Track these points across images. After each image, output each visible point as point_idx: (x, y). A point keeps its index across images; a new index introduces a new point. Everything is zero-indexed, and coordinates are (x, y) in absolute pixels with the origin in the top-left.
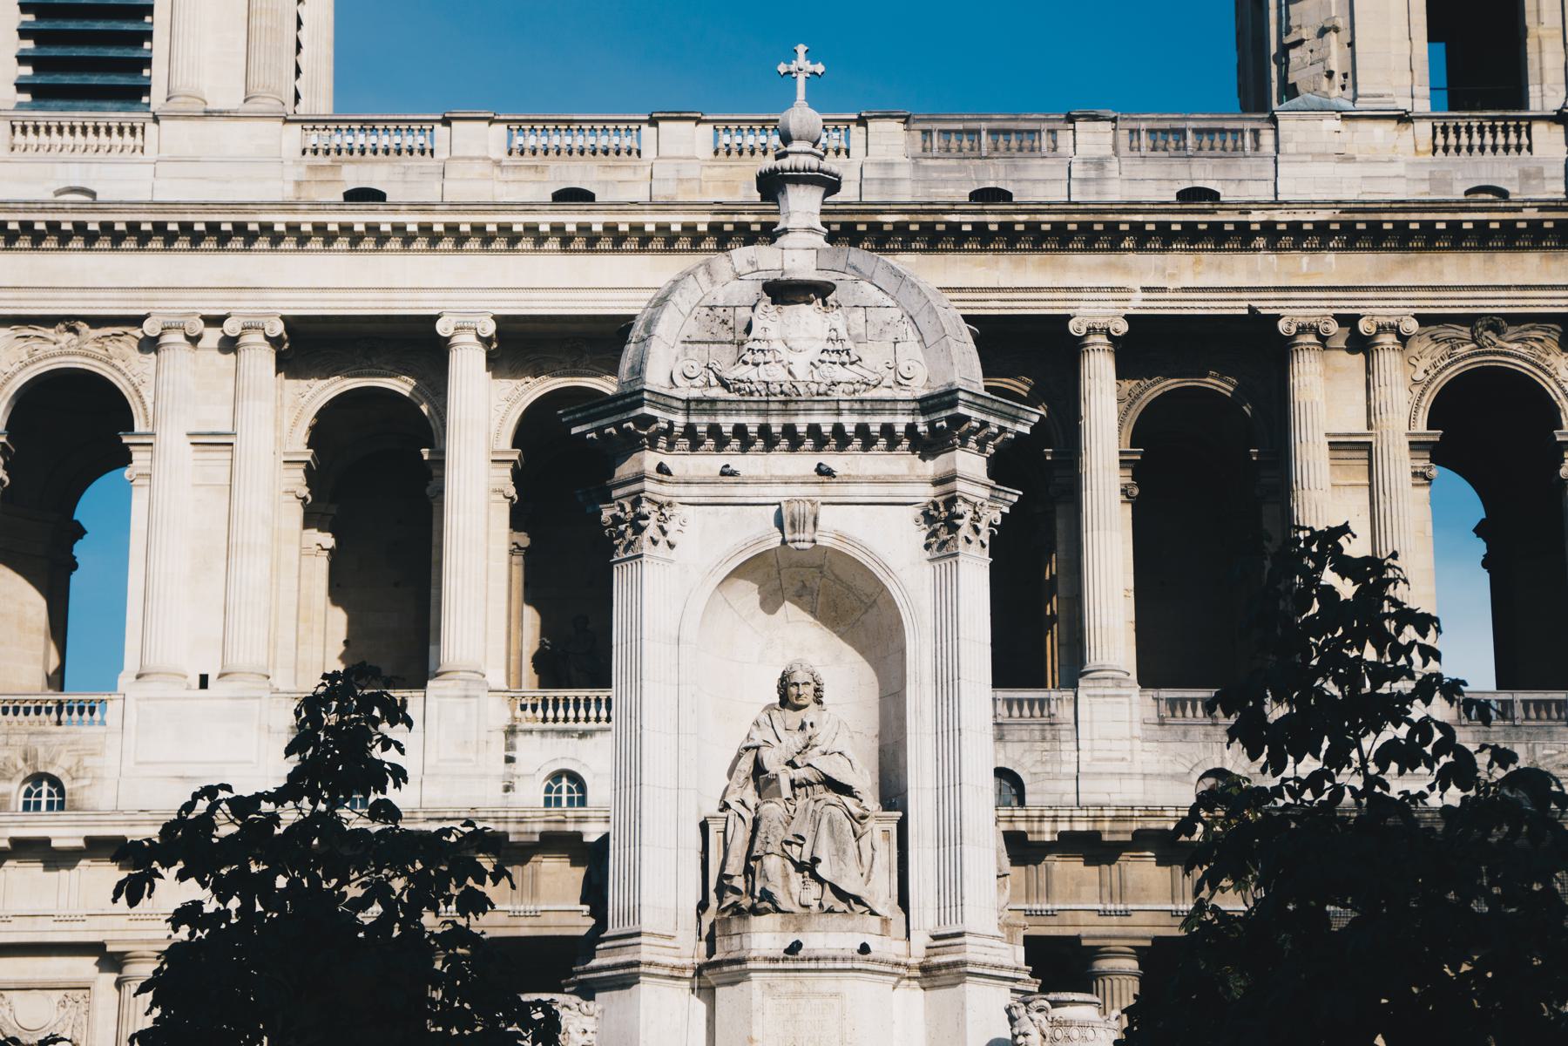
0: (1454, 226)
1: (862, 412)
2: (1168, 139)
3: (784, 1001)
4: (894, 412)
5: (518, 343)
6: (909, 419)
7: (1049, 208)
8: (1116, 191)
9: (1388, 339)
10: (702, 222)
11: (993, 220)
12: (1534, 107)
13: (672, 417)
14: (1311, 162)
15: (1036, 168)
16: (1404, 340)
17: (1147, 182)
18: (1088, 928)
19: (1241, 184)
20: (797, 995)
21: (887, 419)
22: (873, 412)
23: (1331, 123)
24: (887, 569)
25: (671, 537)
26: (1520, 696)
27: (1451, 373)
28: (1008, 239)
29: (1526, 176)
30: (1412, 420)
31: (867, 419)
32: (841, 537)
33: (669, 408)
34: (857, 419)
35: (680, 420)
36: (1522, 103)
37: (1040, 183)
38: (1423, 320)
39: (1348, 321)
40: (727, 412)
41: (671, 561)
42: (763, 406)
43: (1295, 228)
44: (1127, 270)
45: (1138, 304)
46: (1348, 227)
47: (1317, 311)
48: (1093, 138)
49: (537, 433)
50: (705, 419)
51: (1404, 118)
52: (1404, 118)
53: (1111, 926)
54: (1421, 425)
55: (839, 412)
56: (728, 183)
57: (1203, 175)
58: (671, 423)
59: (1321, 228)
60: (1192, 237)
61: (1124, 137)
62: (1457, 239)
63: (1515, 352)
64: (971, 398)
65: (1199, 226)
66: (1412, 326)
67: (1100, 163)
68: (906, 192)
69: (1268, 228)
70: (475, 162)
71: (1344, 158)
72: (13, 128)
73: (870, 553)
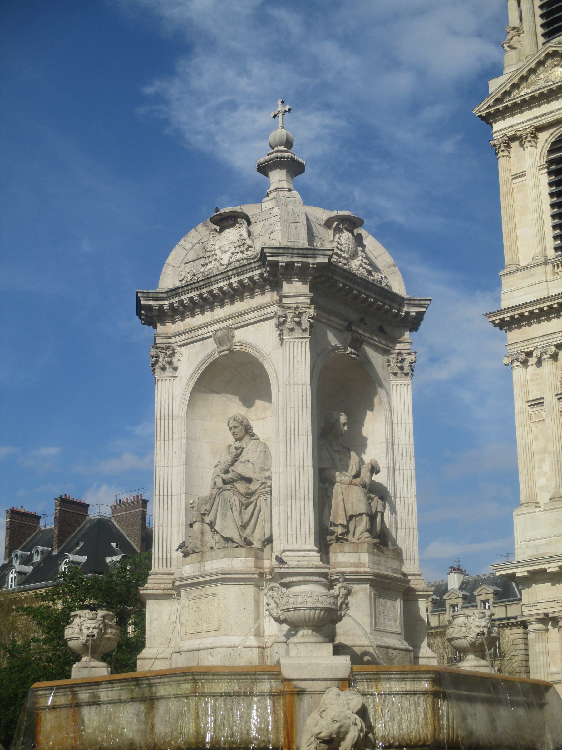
1: (238, 274)
3: (194, 601)
4: (252, 270)
6: (259, 272)
13: (161, 303)
20: (198, 597)
21: (250, 275)
22: (243, 273)
24: (262, 355)
25: (175, 364)
31: (242, 277)
32: (243, 344)
33: (158, 299)
34: (237, 279)
35: (166, 303)
40: (184, 293)
41: (176, 377)
42: (197, 285)
50: (177, 299)
55: (229, 278)
58: (161, 307)
64: (274, 251)
72: (554, 266)
73: (255, 349)
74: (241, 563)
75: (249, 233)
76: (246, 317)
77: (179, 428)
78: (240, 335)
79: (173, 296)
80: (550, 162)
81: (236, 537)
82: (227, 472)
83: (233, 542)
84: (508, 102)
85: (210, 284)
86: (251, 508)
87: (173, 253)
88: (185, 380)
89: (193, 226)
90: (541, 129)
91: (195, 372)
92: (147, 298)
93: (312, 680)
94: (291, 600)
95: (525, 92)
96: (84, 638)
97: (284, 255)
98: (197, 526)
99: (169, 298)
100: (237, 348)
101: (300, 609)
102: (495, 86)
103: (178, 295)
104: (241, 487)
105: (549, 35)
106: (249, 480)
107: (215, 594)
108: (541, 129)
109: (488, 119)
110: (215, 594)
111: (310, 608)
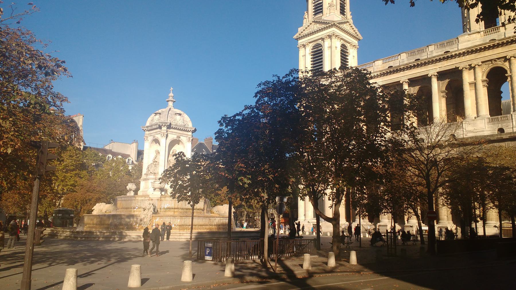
0: (485, 47)
2: (442, 45)
7: (426, 59)
8: (435, 54)
9: (477, 66)
15: (424, 54)
19: (453, 49)
27: (489, 69)
29: (499, 36)
30: (482, 77)
37: (424, 57)
38: (482, 62)
39: (470, 65)
44: (437, 65)
45: (439, 70)
47: (466, 65)
48: (431, 48)
51: (479, 32)
52: (479, 32)
56: (383, 67)
57: (448, 49)
60: (448, 58)
61: (436, 47)
62: (489, 48)
63: (500, 64)
66: (481, 63)
67: (432, 51)
68: (406, 62)
71: (469, 41)
80: (312, 52)
84: (302, 35)
90: (310, 43)
95: (306, 32)
102: (300, 29)
105: (315, 15)
108: (310, 43)
109: (297, 39)
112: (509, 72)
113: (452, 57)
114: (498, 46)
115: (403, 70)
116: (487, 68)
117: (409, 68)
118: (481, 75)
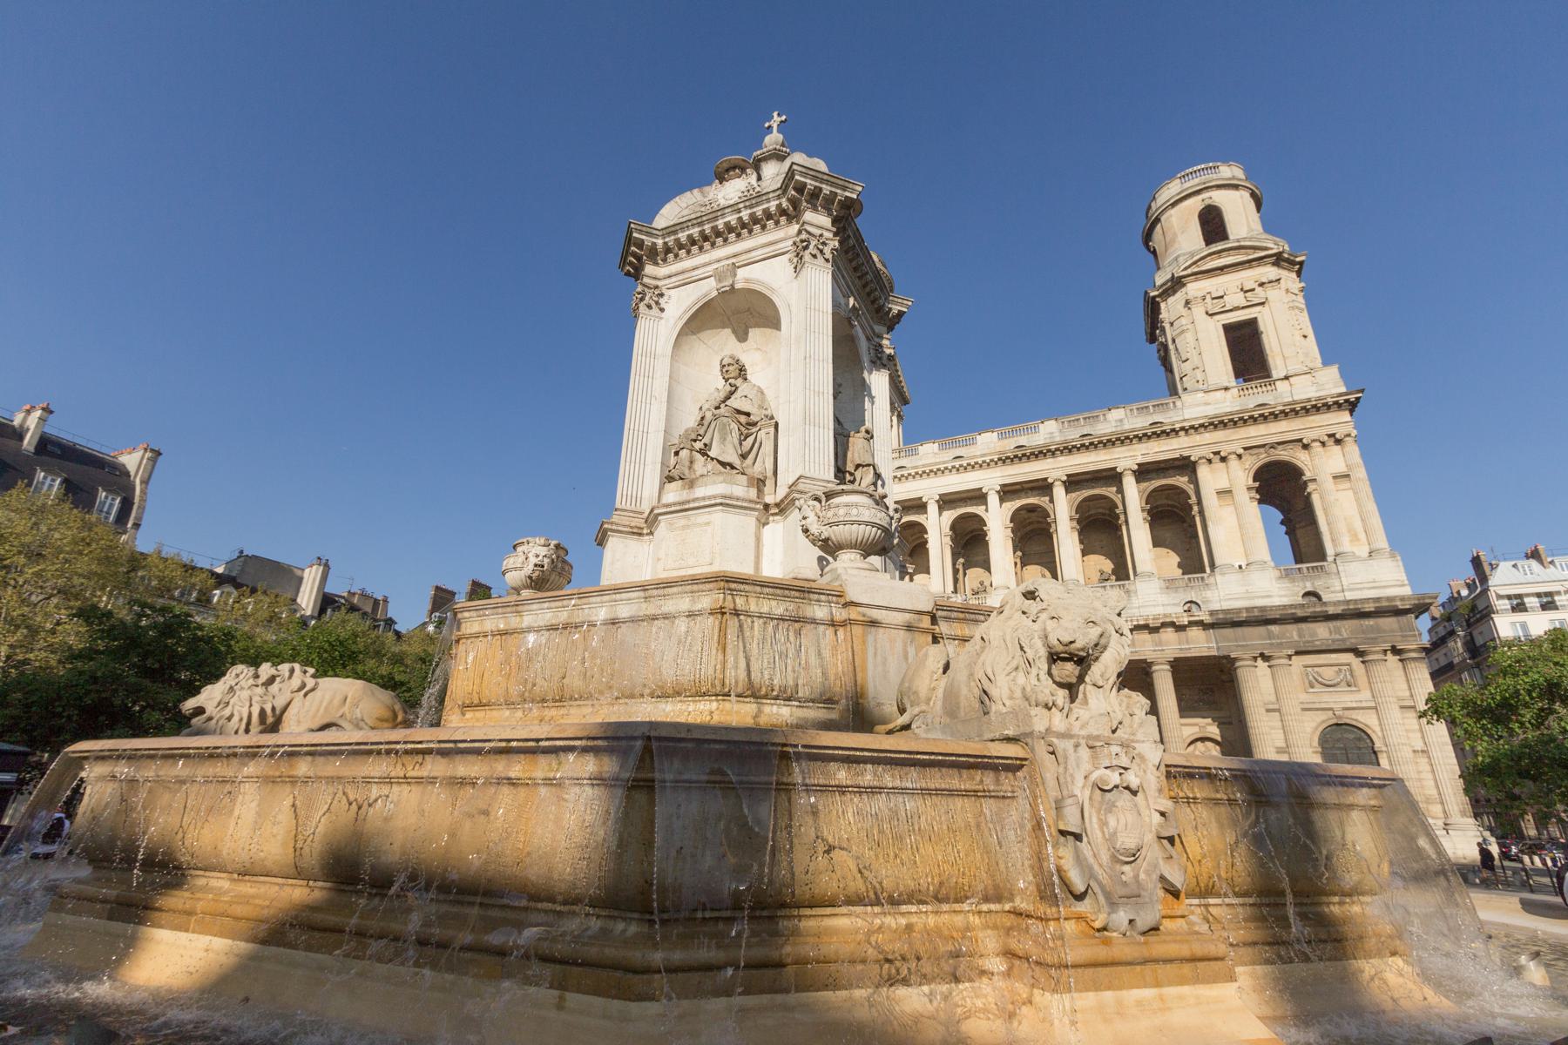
1: (751, 207)
4: (768, 200)
5: (946, 502)
8: (1127, 426)
9: (1233, 457)
10: (996, 458)
11: (1087, 442)
12: (1275, 376)
14: (1192, 407)
16: (1240, 456)
17: (1139, 422)
18: (1149, 656)
19: (1169, 418)
20: (684, 527)
22: (757, 204)
23: (1201, 395)
24: (772, 290)
26: (1304, 566)
28: (1093, 446)
32: (747, 281)
33: (649, 234)
36: (1269, 376)
40: (682, 229)
43: (1192, 427)
45: (1140, 460)
46: (1211, 424)
49: (955, 526)
51: (1226, 389)
52: (1226, 389)
53: (1159, 654)
54: (1250, 482)
55: (739, 211)
58: (654, 244)
59: (1202, 425)
60: (1157, 435)
63: (1283, 455)
65: (1159, 433)
68: (1057, 439)
69: (1182, 429)
70: (929, 453)
71: (1207, 404)
74: (740, 489)
75: (759, 178)
76: (753, 254)
77: (663, 367)
78: (741, 273)
79: (669, 234)
81: (736, 461)
82: (717, 408)
83: (733, 467)
85: (716, 219)
86: (750, 440)
87: (668, 206)
88: (672, 322)
89: (690, 189)
91: (685, 312)
92: (640, 232)
93: (887, 608)
94: (842, 512)
96: (531, 567)
97: (815, 178)
98: (684, 453)
99: (663, 236)
100: (738, 286)
101: (853, 523)
103: (675, 232)
104: (743, 419)
106: (748, 414)
107: (708, 524)
110: (708, 524)
111: (867, 523)
112: (1308, 475)
113: (1166, 434)
114: (1275, 416)
115: (1053, 453)
116: (1254, 462)
117: (1068, 449)
118: (1240, 476)
